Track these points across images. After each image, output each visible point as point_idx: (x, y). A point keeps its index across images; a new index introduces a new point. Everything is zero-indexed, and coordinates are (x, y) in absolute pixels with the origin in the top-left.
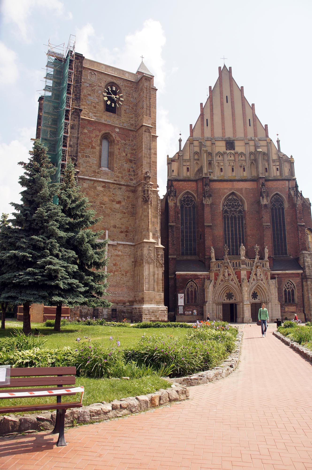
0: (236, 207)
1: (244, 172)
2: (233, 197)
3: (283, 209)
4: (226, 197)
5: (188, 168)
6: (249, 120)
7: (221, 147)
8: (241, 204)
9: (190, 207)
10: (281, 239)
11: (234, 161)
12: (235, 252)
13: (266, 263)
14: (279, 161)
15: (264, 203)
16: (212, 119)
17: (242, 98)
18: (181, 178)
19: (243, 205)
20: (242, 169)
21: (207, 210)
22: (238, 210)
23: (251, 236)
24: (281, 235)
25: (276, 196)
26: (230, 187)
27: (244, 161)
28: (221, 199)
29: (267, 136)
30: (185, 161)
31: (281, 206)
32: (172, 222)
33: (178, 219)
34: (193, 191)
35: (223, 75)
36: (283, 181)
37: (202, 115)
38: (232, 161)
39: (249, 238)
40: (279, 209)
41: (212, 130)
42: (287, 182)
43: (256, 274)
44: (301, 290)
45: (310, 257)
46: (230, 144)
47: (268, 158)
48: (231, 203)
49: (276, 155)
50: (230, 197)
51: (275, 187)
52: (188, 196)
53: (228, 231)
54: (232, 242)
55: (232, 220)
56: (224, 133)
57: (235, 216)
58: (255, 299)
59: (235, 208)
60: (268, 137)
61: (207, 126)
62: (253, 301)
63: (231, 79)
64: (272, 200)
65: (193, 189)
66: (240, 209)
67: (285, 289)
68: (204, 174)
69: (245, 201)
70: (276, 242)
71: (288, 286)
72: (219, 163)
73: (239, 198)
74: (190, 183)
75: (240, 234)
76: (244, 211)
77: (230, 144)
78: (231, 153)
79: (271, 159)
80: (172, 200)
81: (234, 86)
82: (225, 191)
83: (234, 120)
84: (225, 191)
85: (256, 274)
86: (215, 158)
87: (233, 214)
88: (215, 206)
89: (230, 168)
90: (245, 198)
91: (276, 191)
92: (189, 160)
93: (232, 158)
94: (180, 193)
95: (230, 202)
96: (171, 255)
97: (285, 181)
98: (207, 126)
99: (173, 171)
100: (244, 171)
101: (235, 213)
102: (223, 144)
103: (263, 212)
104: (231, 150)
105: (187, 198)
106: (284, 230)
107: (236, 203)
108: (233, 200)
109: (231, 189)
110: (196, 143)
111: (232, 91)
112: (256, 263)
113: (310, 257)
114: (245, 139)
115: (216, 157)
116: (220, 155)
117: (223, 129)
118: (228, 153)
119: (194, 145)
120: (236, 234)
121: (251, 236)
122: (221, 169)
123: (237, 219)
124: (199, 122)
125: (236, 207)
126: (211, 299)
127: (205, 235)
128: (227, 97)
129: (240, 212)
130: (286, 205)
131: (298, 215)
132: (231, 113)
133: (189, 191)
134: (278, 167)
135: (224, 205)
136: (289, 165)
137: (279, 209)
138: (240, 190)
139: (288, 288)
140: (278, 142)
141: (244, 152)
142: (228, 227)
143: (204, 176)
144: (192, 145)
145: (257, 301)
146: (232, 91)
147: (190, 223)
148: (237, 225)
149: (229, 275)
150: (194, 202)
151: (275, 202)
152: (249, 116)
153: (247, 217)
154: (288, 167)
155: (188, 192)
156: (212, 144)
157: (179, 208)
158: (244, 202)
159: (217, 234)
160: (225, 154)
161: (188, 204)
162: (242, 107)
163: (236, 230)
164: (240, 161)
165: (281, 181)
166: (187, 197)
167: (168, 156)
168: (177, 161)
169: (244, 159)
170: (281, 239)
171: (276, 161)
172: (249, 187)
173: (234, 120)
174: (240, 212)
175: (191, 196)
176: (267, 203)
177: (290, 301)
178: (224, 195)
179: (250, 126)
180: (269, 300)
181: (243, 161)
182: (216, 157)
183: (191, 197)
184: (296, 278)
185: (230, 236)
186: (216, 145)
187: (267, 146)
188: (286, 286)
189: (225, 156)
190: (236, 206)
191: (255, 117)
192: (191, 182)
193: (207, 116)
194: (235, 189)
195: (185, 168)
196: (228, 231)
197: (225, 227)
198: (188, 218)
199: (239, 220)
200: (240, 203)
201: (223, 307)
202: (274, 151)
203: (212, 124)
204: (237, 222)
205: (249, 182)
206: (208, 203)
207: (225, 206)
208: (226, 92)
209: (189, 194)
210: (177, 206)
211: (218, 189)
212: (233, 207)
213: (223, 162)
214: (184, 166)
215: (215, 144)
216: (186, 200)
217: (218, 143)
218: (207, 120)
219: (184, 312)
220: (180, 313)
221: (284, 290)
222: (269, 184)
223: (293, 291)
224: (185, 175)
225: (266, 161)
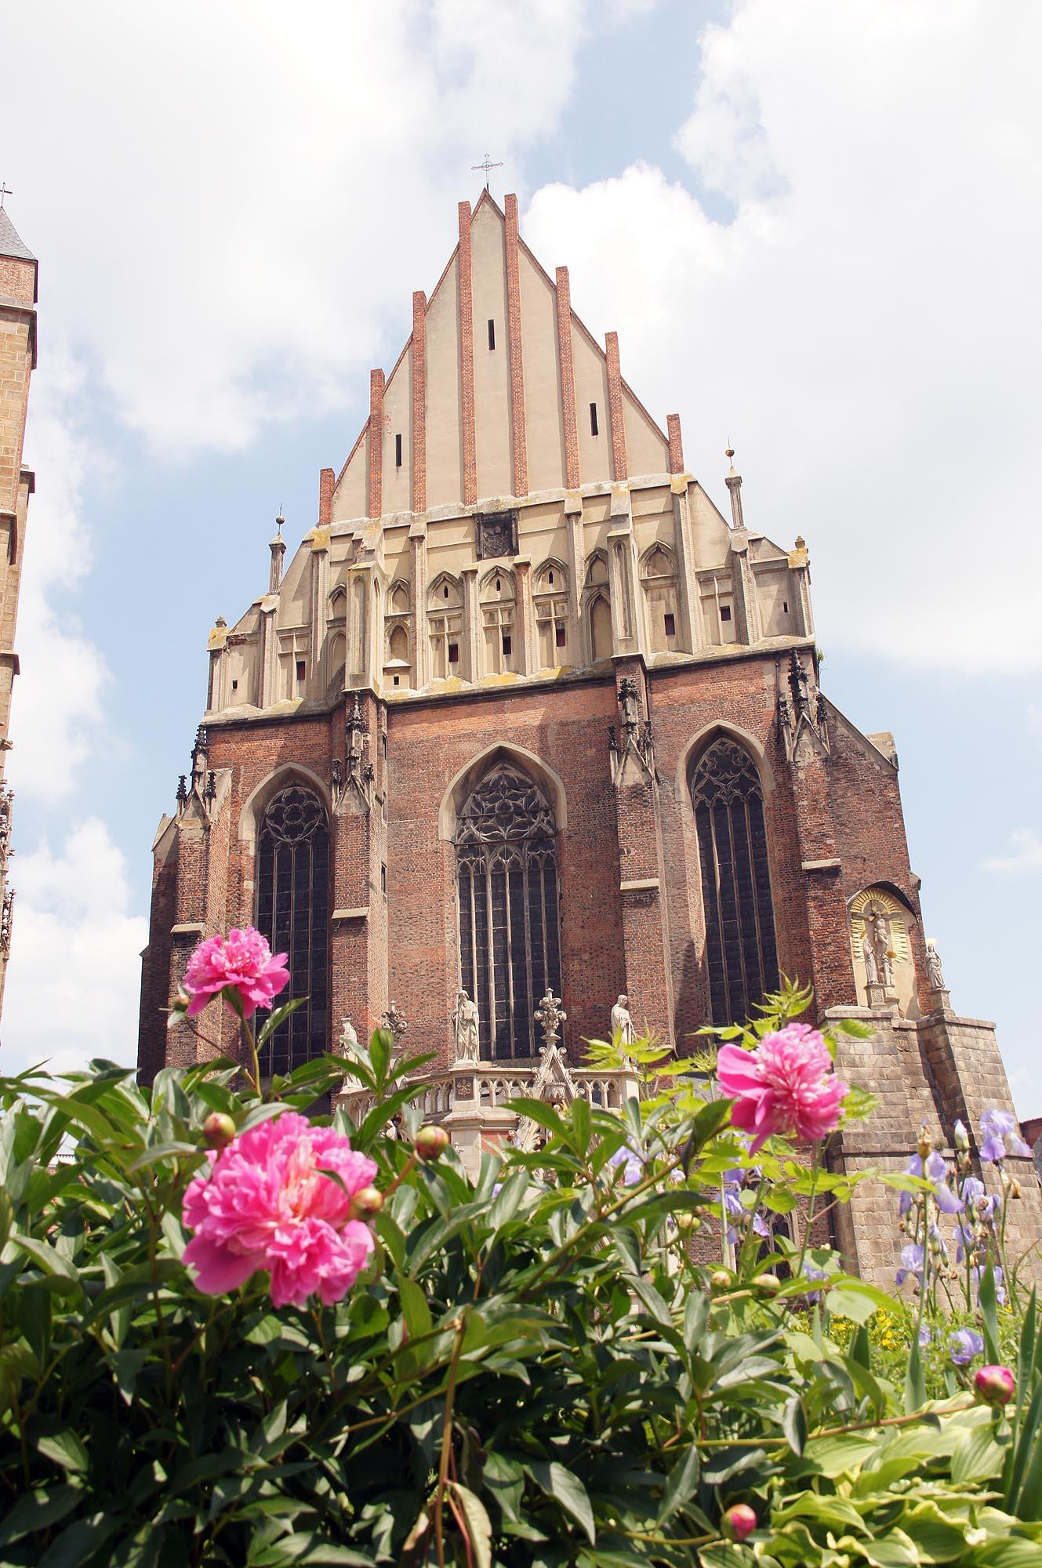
0: (519, 819)
2: (507, 773)
3: (756, 802)
4: (466, 777)
6: (593, 407)
8: (544, 802)
9: (302, 844)
10: (750, 956)
12: (513, 1039)
13: (617, 1084)
14: (730, 572)
15: (630, 783)
17: (558, 316)
19: (550, 809)
22: (530, 831)
23: (586, 957)
24: (749, 935)
25: (723, 744)
27: (561, 597)
29: (675, 467)
31: (744, 792)
35: (476, 231)
36: (746, 665)
37: (375, 424)
38: (502, 606)
39: (577, 967)
40: (737, 804)
41: (417, 481)
49: (718, 548)
50: (493, 776)
52: (295, 792)
59: (519, 826)
60: (681, 469)
61: (399, 463)
63: (512, 244)
64: (699, 767)
65: (315, 755)
66: (540, 829)
68: (347, 679)
70: (725, 976)
73: (535, 775)
75: (537, 950)
76: (557, 833)
78: (497, 572)
81: (527, 277)
82: (465, 746)
84: (465, 746)
87: (506, 854)
88: (411, 826)
90: (559, 771)
91: (713, 719)
94: (253, 785)
95: (493, 800)
98: (399, 463)
99: (235, 684)
101: (511, 848)
103: (623, 827)
104: (501, 556)
105: (289, 800)
106: (766, 910)
107: (522, 802)
108: (504, 788)
109: (489, 736)
111: (510, 297)
114: (571, 496)
116: (450, 587)
117: (468, 465)
121: (586, 957)
122: (454, 651)
123: (525, 878)
124: (362, 453)
125: (519, 819)
128: (491, 324)
129: (541, 839)
130: (768, 784)
131: (807, 822)
132: (504, 392)
134: (729, 602)
136: (784, 584)
137: (737, 804)
140: (733, 484)
142: (482, 918)
143: (348, 687)
146: (510, 297)
147: (301, 919)
148: (526, 903)
150: (324, 820)
151: (713, 773)
152: (589, 388)
153: (566, 860)
155: (291, 771)
158: (555, 789)
159: (418, 960)
160: (470, 576)
161: (293, 831)
162: (560, 355)
166: (294, 797)
167: (220, 623)
170: (750, 956)
172: (577, 713)
174: (541, 840)
175: (307, 789)
178: (459, 765)
179: (595, 432)
181: (557, 598)
183: (310, 797)
189: (473, 587)
190: (519, 812)
191: (617, 389)
192: (307, 726)
193: (398, 421)
194: (510, 735)
198: (293, 897)
199: (535, 883)
200: (540, 797)
202: (709, 529)
203: (418, 453)
204: (526, 889)
205: (577, 692)
208: (488, 304)
209: (298, 782)
211: (427, 741)
212: (505, 821)
213: (460, 616)
216: (287, 809)
222: (680, 691)
225: (669, 582)
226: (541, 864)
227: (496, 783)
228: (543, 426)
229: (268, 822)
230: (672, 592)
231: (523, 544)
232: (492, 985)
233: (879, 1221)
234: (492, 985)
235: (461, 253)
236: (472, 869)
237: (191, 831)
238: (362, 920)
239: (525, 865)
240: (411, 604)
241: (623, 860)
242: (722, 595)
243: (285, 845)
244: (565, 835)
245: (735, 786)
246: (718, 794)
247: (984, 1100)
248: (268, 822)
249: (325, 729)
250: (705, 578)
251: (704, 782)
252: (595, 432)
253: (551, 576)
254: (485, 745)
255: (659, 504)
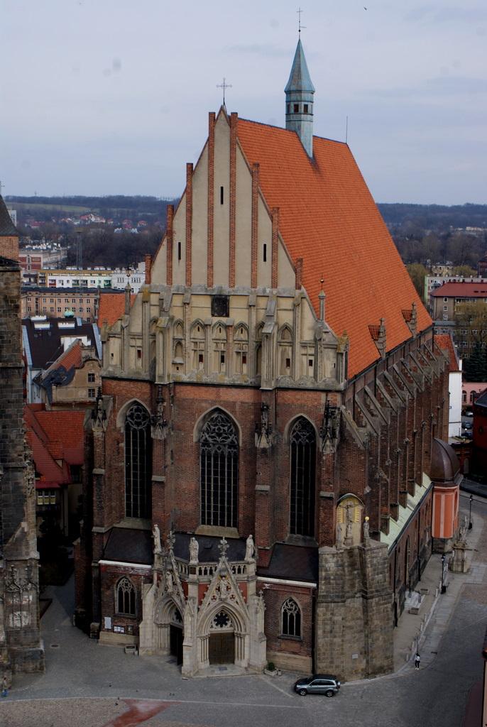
1: (245, 366)
4: (204, 417)
5: (139, 351)
6: (265, 245)
7: (202, 309)
9: (141, 430)
11: (225, 342)
15: (262, 447)
16: (189, 243)
18: (124, 375)
19: (237, 433)
20: (240, 358)
21: (157, 450)
22: (229, 440)
26: (212, 397)
28: (195, 421)
30: (134, 337)
32: (100, 467)
33: (119, 453)
34: (145, 401)
35: (217, 131)
42: (323, 395)
43: (219, 587)
44: (311, 617)
45: (335, 559)
46: (221, 304)
47: (293, 337)
48: (216, 428)
50: (215, 415)
51: (299, 402)
53: (209, 480)
54: (216, 501)
55: (216, 459)
56: (210, 276)
57: (222, 452)
58: (221, 626)
59: (224, 438)
61: (180, 258)
62: (218, 629)
67: (285, 610)
69: (240, 427)
71: (292, 605)
72: (197, 343)
74: (139, 384)
77: (221, 304)
78: (220, 324)
79: (298, 341)
80: (99, 426)
82: (204, 405)
83: (232, 248)
84: (204, 405)
85: (219, 589)
86: (187, 334)
87: (219, 448)
89: (218, 355)
90: (239, 422)
92: (140, 337)
93: (223, 335)
95: (215, 426)
96: (97, 526)
97: (318, 393)
98: (180, 258)
99: (112, 355)
100: (244, 360)
102: (206, 303)
103: (258, 464)
107: (226, 428)
109: (214, 402)
110: (154, 299)
111: (232, 175)
112: (220, 571)
113: (335, 559)
115: (191, 330)
117: (210, 267)
118: (215, 325)
119: (152, 303)
120: (223, 488)
122: (201, 358)
123: (226, 459)
126: (150, 617)
127: (153, 498)
128: (222, 188)
132: (227, 229)
133: (138, 400)
134: (312, 358)
135: (200, 430)
138: (232, 405)
139: (290, 610)
141: (245, 321)
144: (147, 305)
145: (226, 629)
146: (232, 175)
149: (174, 584)
154: (332, 359)
155: (135, 402)
156: (185, 304)
157: (123, 431)
159: (184, 487)
163: (223, 481)
164: (236, 342)
165: (312, 393)
168: (119, 336)
169: (246, 339)
171: (308, 345)
173: (232, 248)
176: (267, 446)
177: (292, 633)
179: (265, 260)
180: (245, 630)
181: (243, 342)
182: (191, 330)
184: (304, 596)
185: (212, 490)
186: (194, 305)
187: (293, 310)
188: (287, 604)
189: (209, 330)
195: (133, 352)
196: (209, 480)
197: (203, 471)
201: (171, 630)
206: (159, 438)
207: (206, 434)
208: (222, 179)
210: (116, 428)
212: (219, 435)
214: (132, 346)
215: (188, 304)
217: (196, 301)
218: (180, 244)
219: (113, 627)
220: (106, 627)
221: (283, 611)
222: (288, 396)
223: (298, 615)
224: (133, 366)
226: (232, 455)
227: (216, 418)
228: (244, 251)
229: (128, 419)
230: (290, 348)
231: (232, 312)
232: (212, 498)
233: (327, 624)
234: (212, 498)
235: (210, 142)
236: (206, 452)
237: (98, 433)
238: (162, 483)
239: (226, 454)
240: (184, 335)
241: (258, 477)
242: (310, 355)
243: (135, 431)
244: (241, 449)
245: (307, 438)
246: (300, 440)
247: (376, 576)
248: (128, 419)
249: (149, 386)
250: (304, 346)
251: (295, 434)
252: (265, 260)
253: (242, 330)
254: (212, 406)
255: (287, 304)
